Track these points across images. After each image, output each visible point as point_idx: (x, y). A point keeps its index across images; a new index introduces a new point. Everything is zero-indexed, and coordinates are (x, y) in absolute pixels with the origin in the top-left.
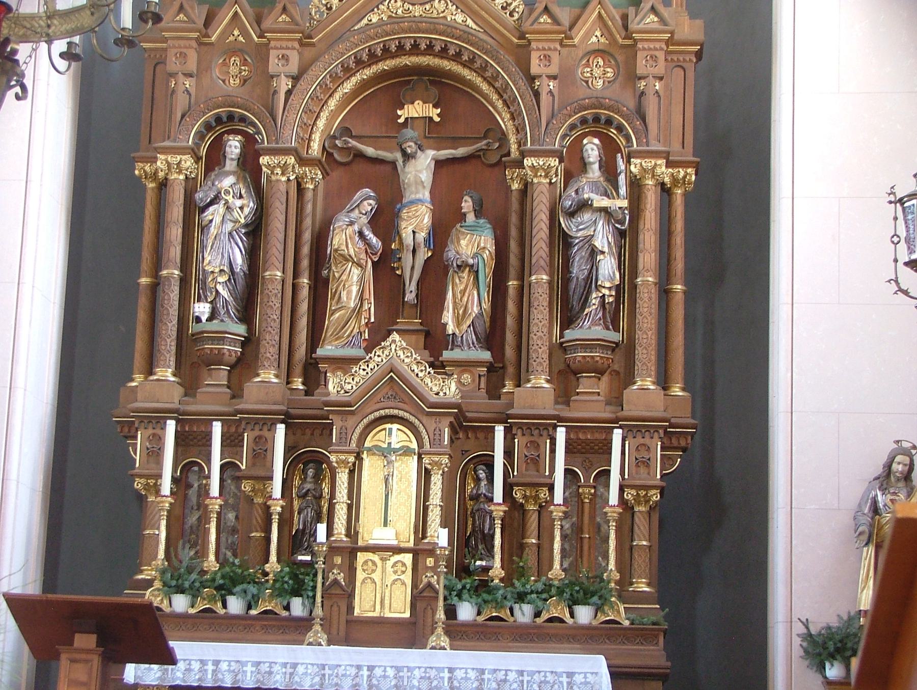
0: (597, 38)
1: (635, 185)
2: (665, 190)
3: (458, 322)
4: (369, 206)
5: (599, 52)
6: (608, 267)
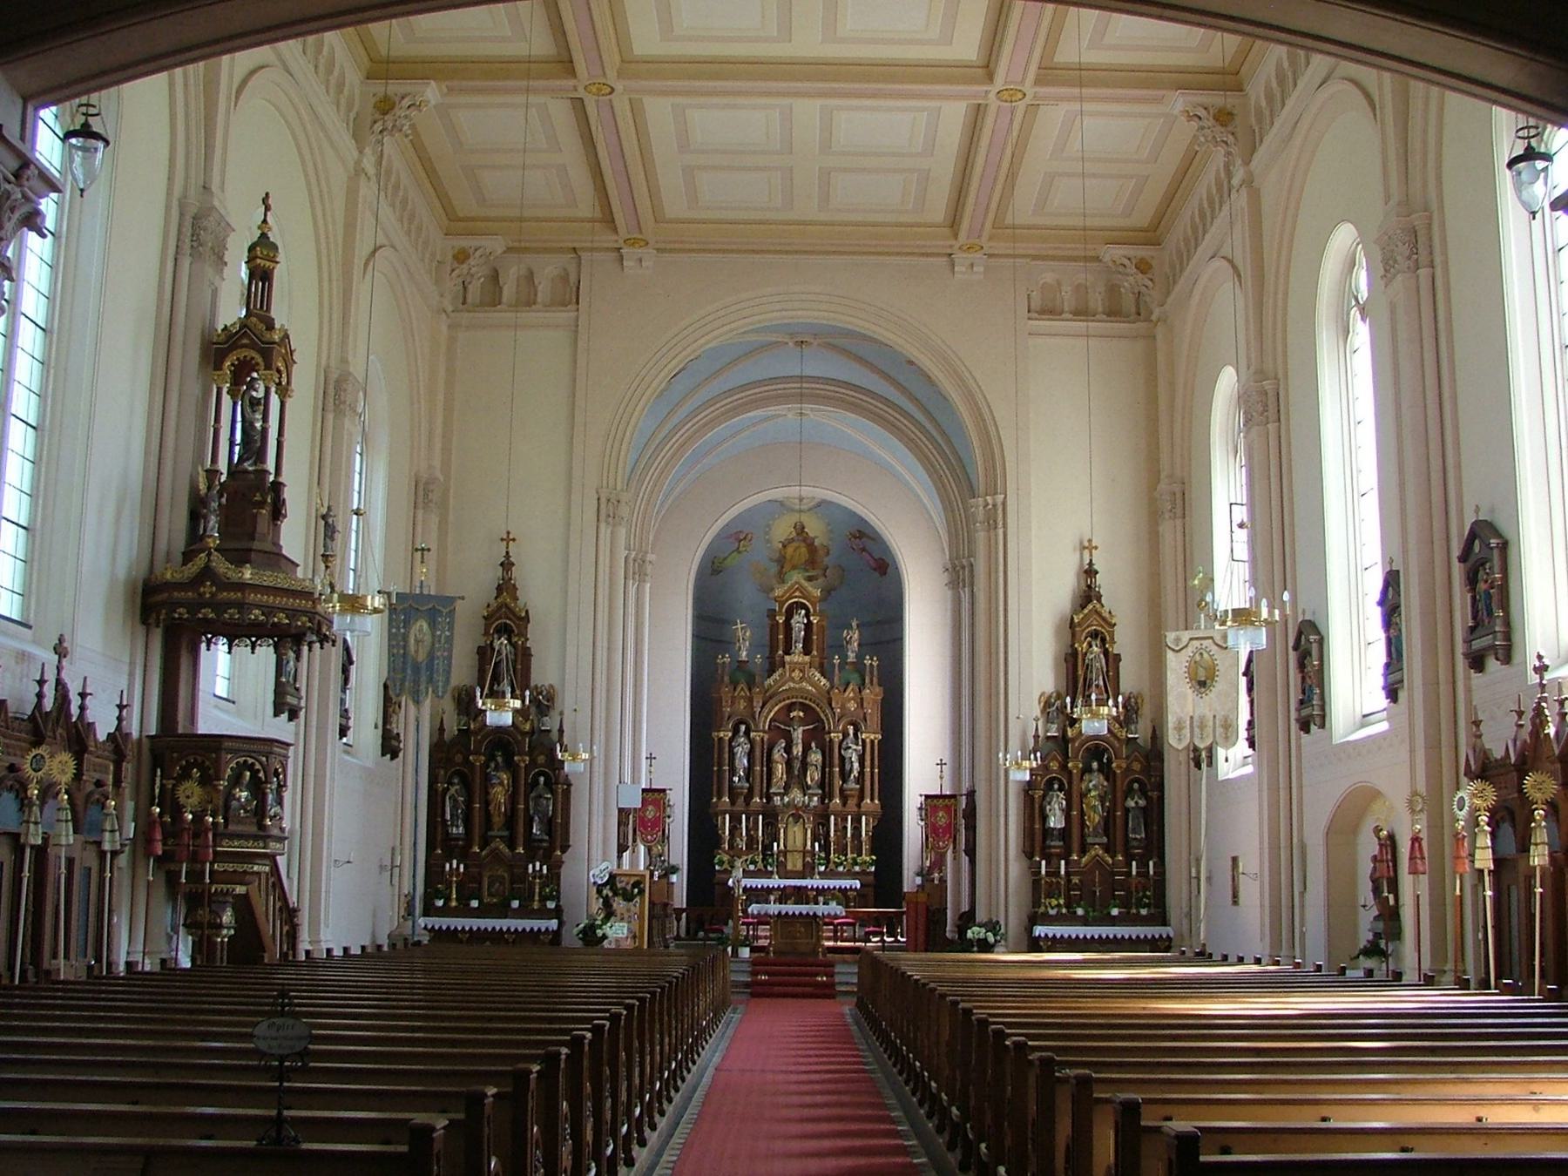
0: (851, 695)
1: (863, 741)
2: (872, 742)
3: (812, 780)
4: (783, 745)
5: (852, 699)
6: (856, 765)
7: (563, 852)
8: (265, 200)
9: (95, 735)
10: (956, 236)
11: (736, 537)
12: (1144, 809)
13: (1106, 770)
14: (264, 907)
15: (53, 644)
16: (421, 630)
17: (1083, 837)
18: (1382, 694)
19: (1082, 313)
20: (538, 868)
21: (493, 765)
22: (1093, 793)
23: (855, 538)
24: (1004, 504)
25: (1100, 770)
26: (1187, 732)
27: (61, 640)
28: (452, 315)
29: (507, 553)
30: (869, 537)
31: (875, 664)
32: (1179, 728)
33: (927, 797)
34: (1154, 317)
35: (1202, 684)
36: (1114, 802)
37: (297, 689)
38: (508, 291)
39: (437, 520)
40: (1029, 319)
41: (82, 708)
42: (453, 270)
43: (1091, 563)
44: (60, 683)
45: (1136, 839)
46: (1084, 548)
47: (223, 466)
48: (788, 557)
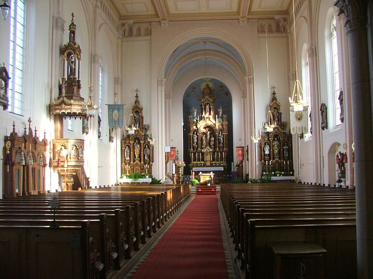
2: (226, 135)
6: (222, 141)
7: (152, 163)
8: (72, 15)
9: (39, 140)
10: (239, 14)
11: (192, 88)
12: (288, 149)
13: (278, 140)
14: (81, 177)
15: (28, 120)
16: (116, 112)
17: (273, 155)
18: (340, 121)
19: (270, 31)
20: (147, 166)
21: (135, 143)
22: (276, 146)
23: (220, 87)
24: (253, 78)
25: (277, 140)
26: (295, 130)
27: (30, 118)
28: (122, 39)
29: (137, 94)
30: (224, 87)
31: (226, 117)
32: (293, 129)
33: (237, 147)
34: (288, 32)
35: (299, 119)
36: (280, 147)
37: (88, 128)
38: (135, 32)
39: (120, 87)
40: (258, 34)
41: (35, 134)
42: (121, 28)
43: (274, 91)
44: (30, 128)
46: (272, 88)
47: (66, 77)
48: (205, 92)
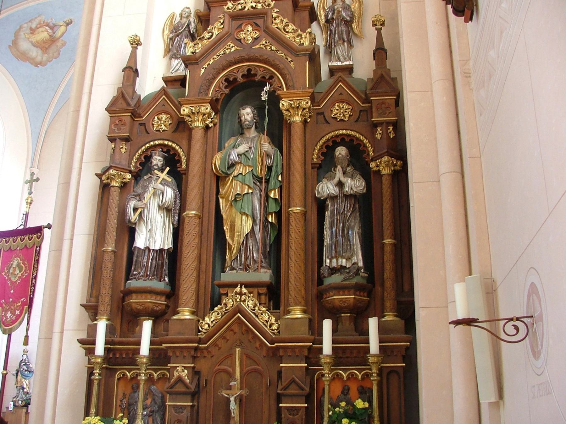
22: (239, 169)
45: (341, 269)
